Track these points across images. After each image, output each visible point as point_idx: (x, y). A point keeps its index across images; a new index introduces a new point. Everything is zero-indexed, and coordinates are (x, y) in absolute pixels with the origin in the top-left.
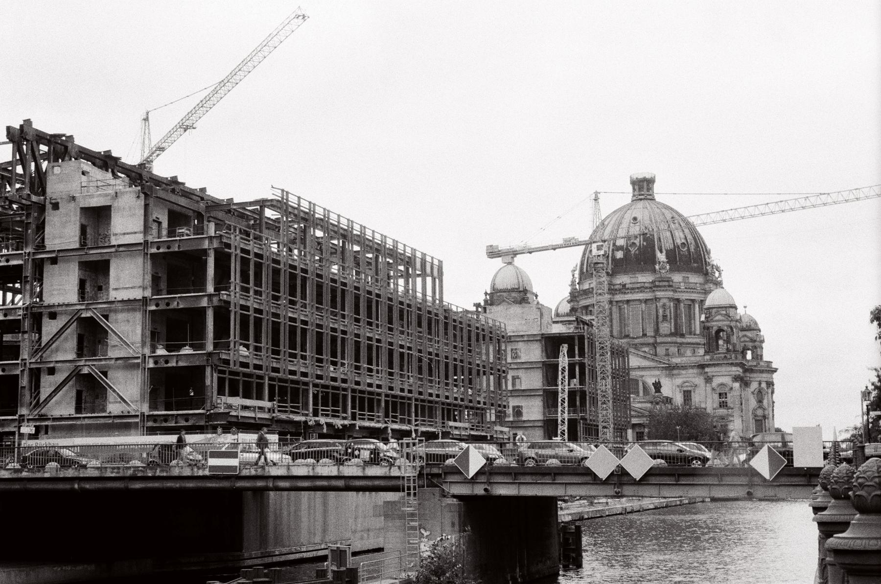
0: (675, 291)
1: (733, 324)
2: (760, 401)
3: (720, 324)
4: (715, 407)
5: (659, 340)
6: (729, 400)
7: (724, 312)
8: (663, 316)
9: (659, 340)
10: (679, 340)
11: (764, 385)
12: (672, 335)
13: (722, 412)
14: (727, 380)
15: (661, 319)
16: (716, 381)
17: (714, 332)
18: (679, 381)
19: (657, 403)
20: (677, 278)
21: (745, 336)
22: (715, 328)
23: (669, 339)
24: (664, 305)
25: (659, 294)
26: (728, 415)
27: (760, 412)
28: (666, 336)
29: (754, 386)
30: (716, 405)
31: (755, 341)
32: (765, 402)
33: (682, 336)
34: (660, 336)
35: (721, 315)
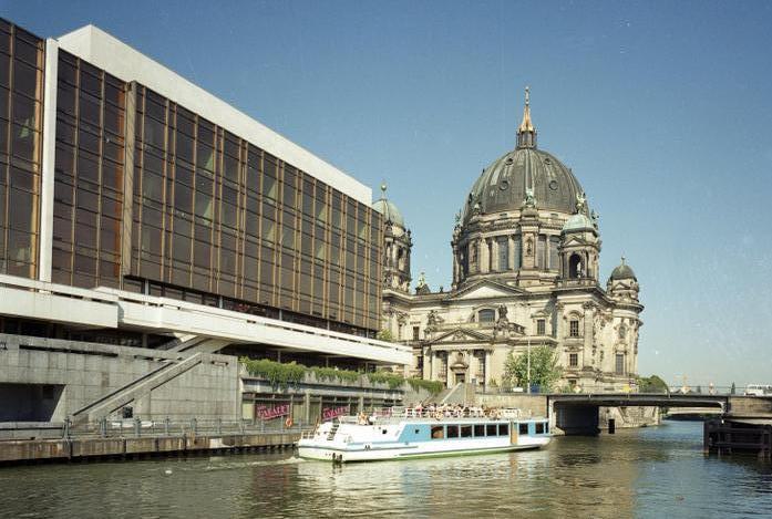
0: (540, 226)
1: (588, 248)
2: (622, 337)
3: (576, 248)
4: (565, 335)
5: (522, 273)
6: (581, 329)
7: (580, 237)
8: (529, 250)
9: (522, 273)
10: (542, 275)
11: (627, 321)
12: (535, 268)
13: (573, 340)
14: (578, 308)
15: (525, 253)
16: (568, 309)
17: (568, 258)
18: (533, 311)
19: (500, 330)
20: (544, 214)
21: (621, 283)
22: (569, 254)
23: (532, 273)
24: (529, 240)
25: (524, 229)
26: (579, 344)
27: (621, 347)
28: (529, 270)
29: (617, 321)
30: (566, 332)
31: (629, 288)
32: (627, 338)
33: (547, 271)
34: (524, 270)
35: (575, 239)
